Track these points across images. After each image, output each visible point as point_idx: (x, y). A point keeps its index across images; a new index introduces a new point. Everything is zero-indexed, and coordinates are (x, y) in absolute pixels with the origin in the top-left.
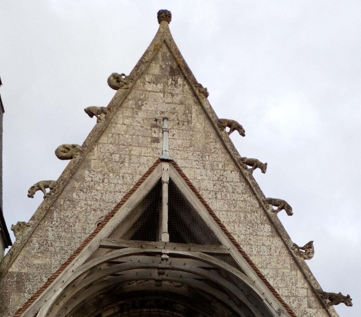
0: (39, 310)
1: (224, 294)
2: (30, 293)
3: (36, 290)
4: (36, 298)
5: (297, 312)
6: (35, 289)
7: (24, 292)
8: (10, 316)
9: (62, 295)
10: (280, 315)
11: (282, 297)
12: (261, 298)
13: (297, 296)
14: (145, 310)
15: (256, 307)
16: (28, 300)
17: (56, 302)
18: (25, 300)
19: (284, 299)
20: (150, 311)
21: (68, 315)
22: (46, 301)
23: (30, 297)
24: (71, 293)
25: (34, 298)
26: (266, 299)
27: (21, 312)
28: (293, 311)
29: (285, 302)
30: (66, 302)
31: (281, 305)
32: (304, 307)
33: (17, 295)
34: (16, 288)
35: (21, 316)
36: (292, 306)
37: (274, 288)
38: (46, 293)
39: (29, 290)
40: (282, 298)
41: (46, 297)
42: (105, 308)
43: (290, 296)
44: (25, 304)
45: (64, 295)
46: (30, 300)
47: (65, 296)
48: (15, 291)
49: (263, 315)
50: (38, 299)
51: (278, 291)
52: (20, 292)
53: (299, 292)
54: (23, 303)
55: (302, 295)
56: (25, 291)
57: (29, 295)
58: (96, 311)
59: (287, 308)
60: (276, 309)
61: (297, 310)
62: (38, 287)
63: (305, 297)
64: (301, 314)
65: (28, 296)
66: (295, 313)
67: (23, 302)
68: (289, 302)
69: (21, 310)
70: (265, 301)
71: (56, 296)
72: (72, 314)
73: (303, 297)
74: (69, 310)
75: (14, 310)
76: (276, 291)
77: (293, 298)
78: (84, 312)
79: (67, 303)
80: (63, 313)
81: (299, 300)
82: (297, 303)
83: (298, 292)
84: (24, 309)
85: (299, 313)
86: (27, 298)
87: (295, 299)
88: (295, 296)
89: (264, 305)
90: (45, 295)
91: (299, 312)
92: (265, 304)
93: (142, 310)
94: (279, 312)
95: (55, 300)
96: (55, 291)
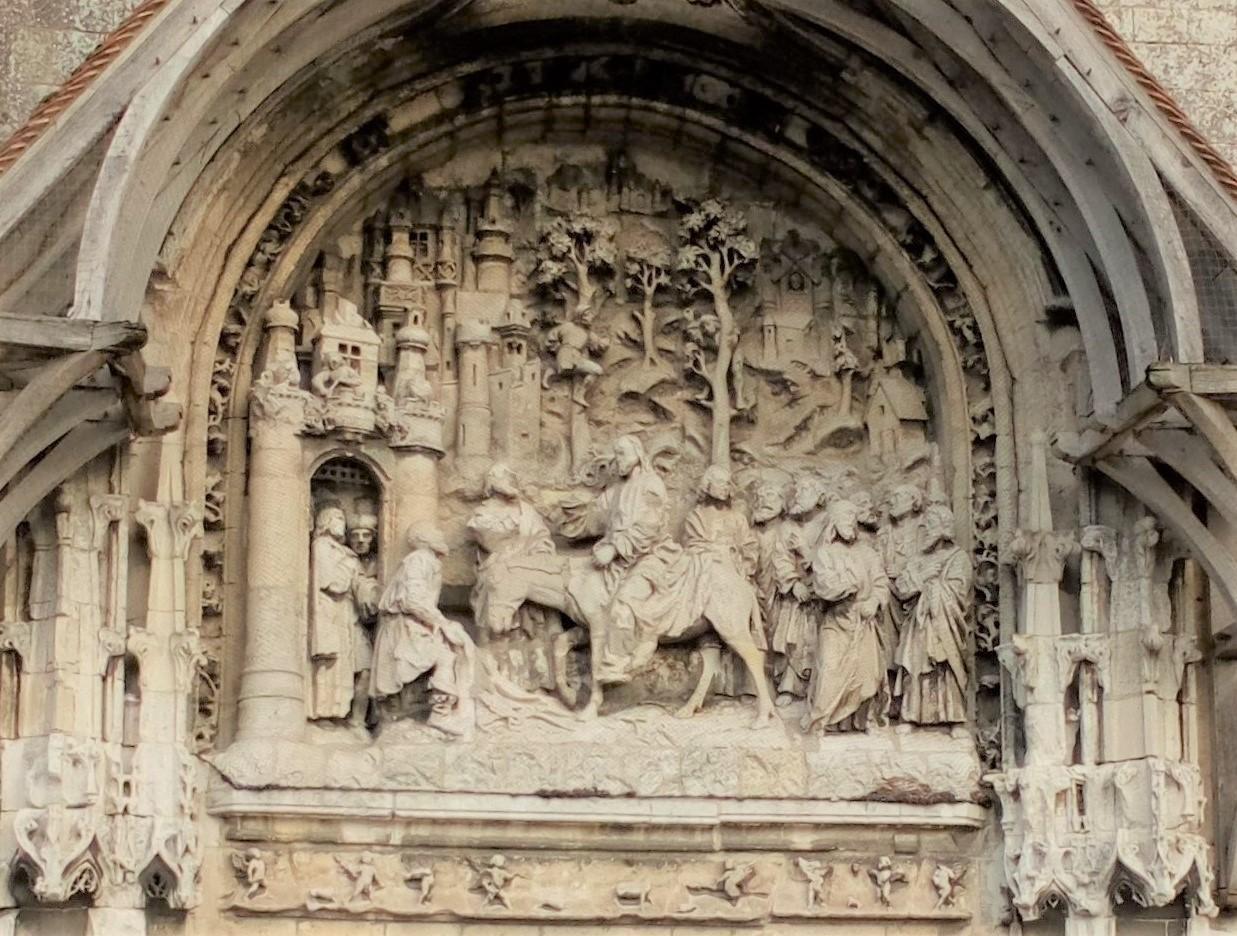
0: (127, 98)
1: (893, 35)
2: (90, 32)
3: (117, 20)
4: (118, 52)
5: (1195, 109)
6: (113, 12)
7: (68, 28)
8: (10, 124)
9: (225, 40)
10: (1125, 120)
11: (1134, 45)
12: (1046, 51)
13: (1195, 43)
14: (566, 100)
15: (1027, 86)
16: (83, 60)
17: (201, 69)
18: (71, 60)
19: (1140, 53)
20: (587, 107)
21: (251, 122)
22: (158, 62)
23: (90, 46)
24: (262, 29)
25: (107, 51)
26: (1066, 56)
27: (56, 108)
28: (1180, 106)
29: (1148, 66)
30: (239, 65)
31: (1130, 81)
32: (1223, 89)
33: (37, 37)
34: (33, 12)
35: (55, 123)
36: (1174, 82)
37: (1100, 9)
38: (157, 30)
39: (87, 17)
40: (1133, 50)
41: (159, 46)
42: (404, 94)
43: (1165, 43)
44: (69, 77)
45: (233, 40)
46: (90, 58)
47: (236, 43)
48: (32, 23)
49: (1054, 119)
50: (127, 53)
51: (1116, 21)
52: (53, 26)
53: (1203, 25)
54: (65, 73)
55: (1216, 37)
56: (73, 21)
57: (87, 39)
58: (364, 105)
59: (1156, 90)
60: (1109, 95)
61: (1197, 100)
62: (124, 5)
63: (1230, 46)
64: (1211, 114)
65: (83, 44)
66: (1187, 114)
67: (63, 68)
68: (1162, 67)
69: (54, 100)
70: (1062, 64)
71: (201, 44)
72: (268, 115)
73: (1222, 48)
74: (254, 99)
75: (26, 102)
76: (1108, 20)
77: (1180, 50)
78: (316, 107)
79: (245, 70)
80: (231, 112)
81: (1204, 60)
82: (1197, 73)
83: (1199, 27)
84: (69, 96)
85: (1204, 114)
86: (81, 52)
87: (1185, 55)
88: (1186, 44)
89: (1057, 79)
90: (152, 37)
91: (1202, 110)
92: (1064, 76)
93: (555, 100)
94: (1122, 108)
95: (196, 61)
96: (195, 21)
